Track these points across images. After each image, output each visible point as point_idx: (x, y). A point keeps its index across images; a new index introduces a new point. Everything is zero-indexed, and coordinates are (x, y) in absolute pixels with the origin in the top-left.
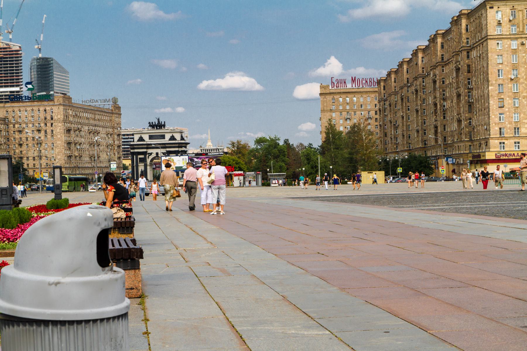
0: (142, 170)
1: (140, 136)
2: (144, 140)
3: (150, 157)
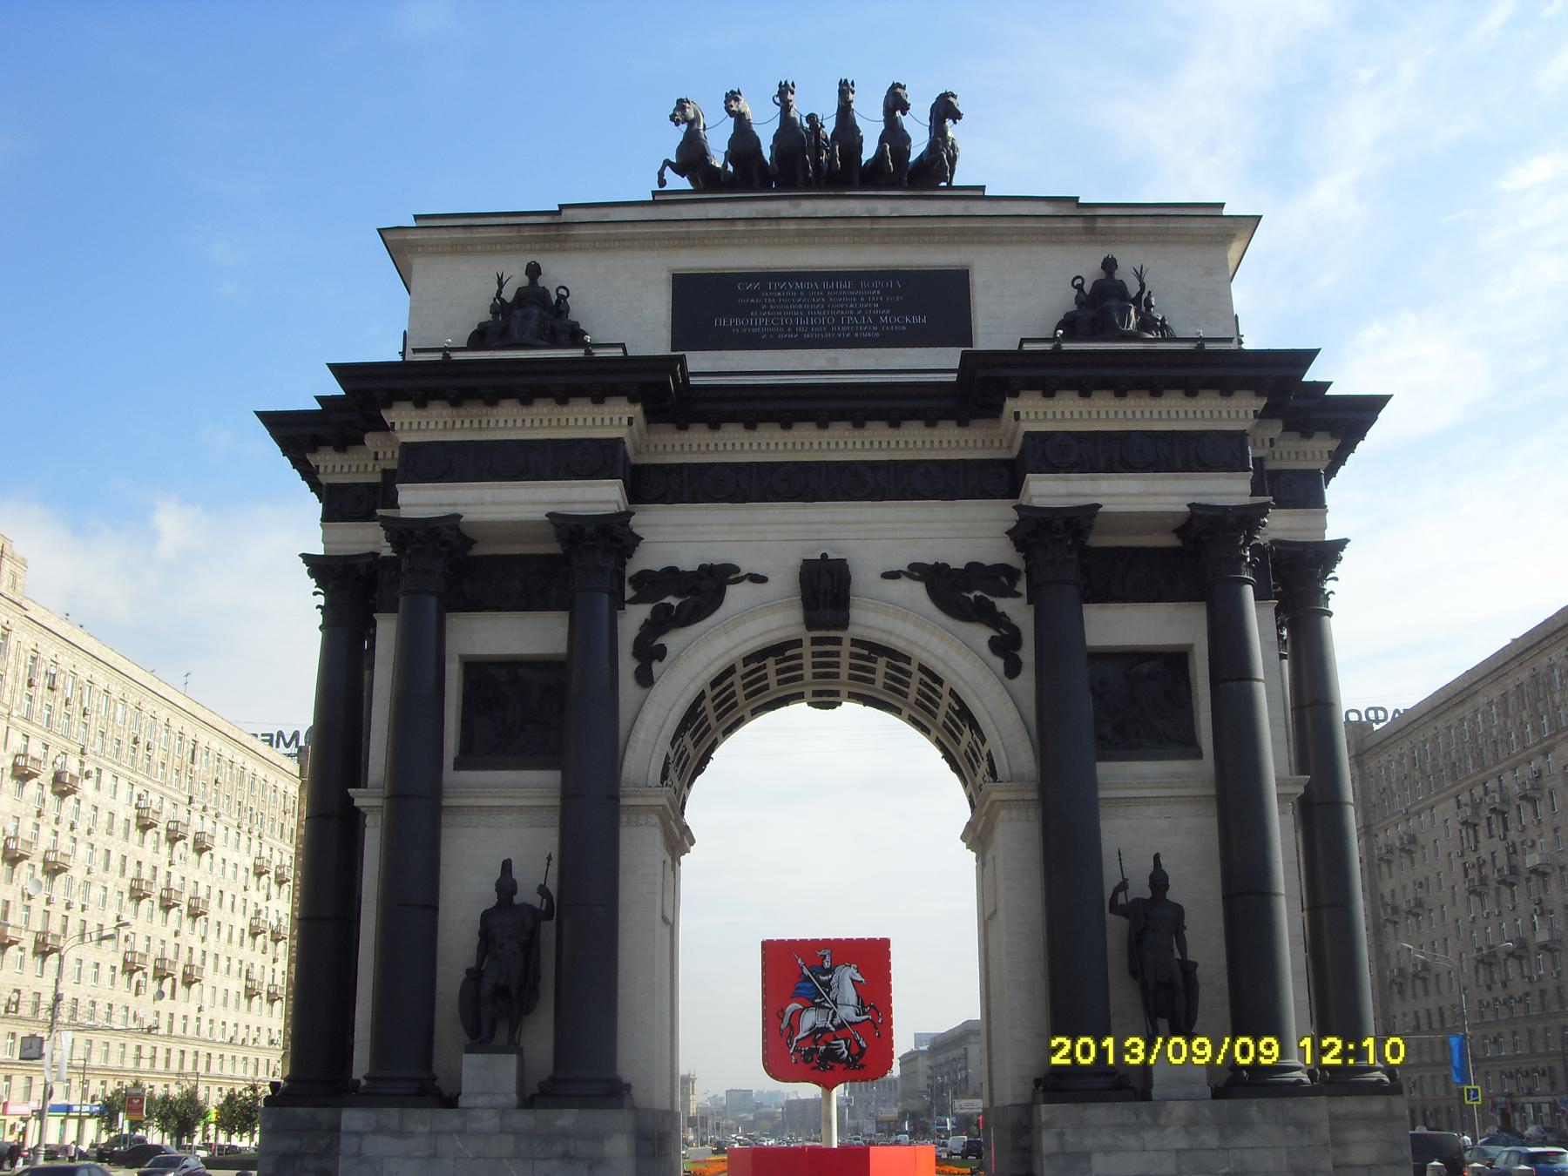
0: (506, 884)
1: (517, 278)
3: (673, 641)
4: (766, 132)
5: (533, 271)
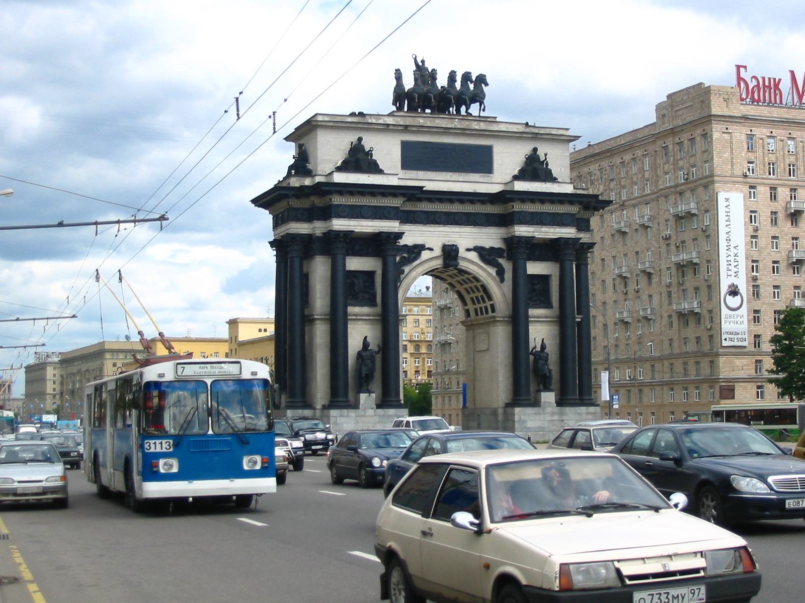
0: (366, 344)
2: (374, 168)
3: (407, 269)
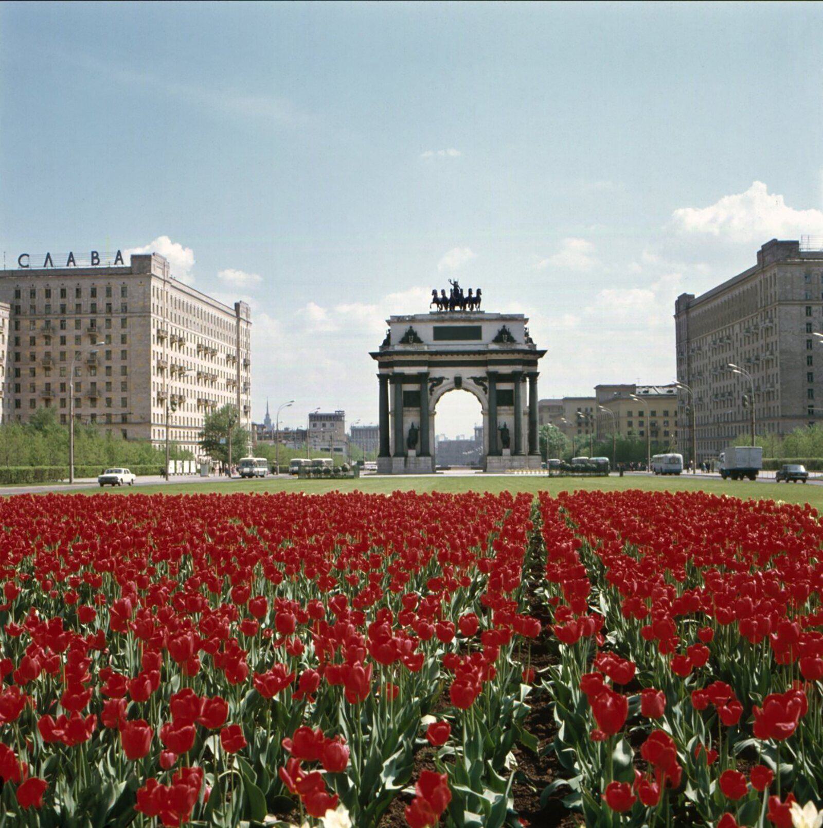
0: (413, 426)
2: (418, 340)
3: (435, 389)
4: (448, 295)
5: (411, 327)
